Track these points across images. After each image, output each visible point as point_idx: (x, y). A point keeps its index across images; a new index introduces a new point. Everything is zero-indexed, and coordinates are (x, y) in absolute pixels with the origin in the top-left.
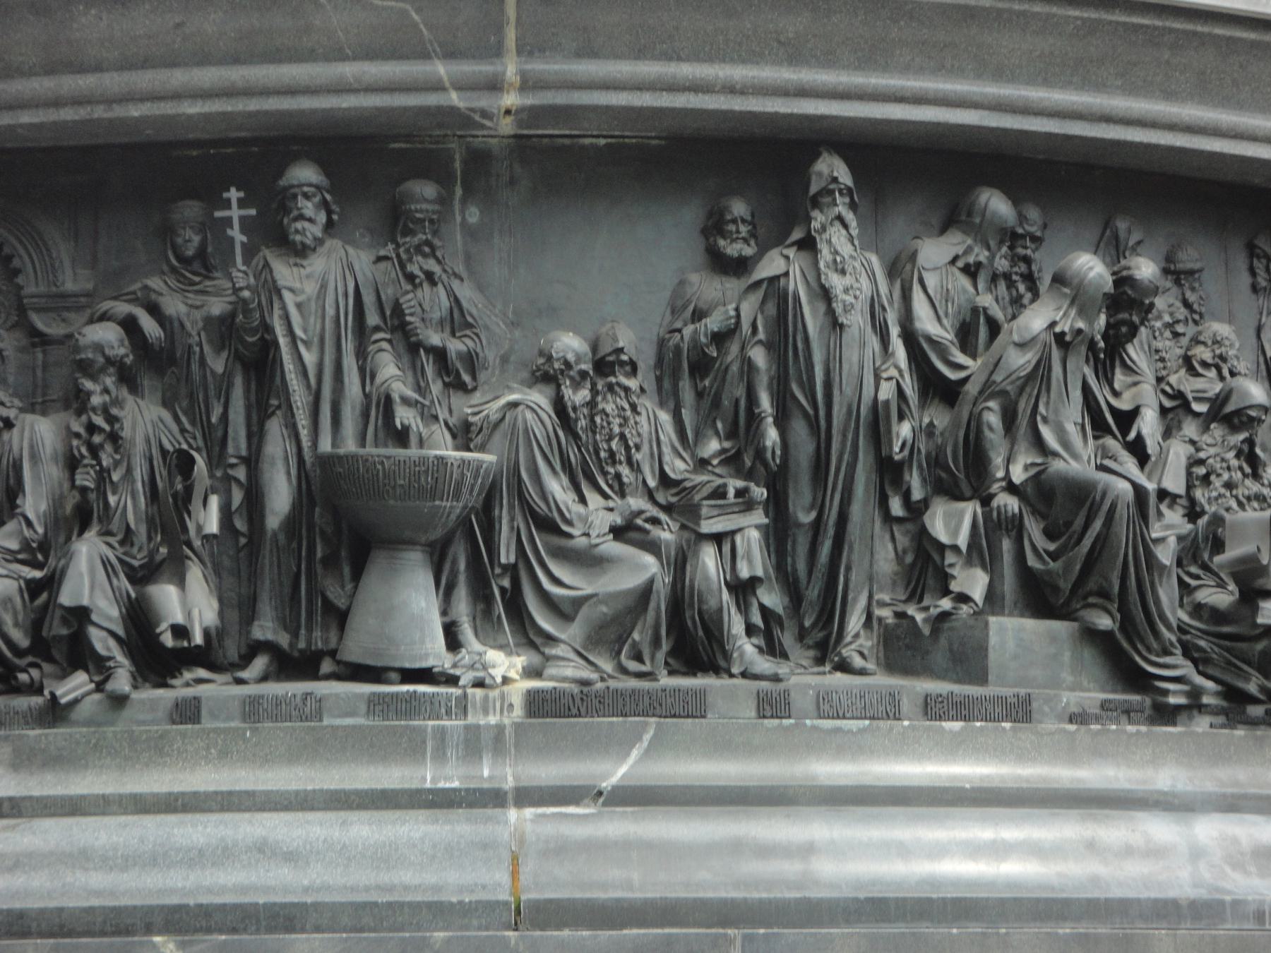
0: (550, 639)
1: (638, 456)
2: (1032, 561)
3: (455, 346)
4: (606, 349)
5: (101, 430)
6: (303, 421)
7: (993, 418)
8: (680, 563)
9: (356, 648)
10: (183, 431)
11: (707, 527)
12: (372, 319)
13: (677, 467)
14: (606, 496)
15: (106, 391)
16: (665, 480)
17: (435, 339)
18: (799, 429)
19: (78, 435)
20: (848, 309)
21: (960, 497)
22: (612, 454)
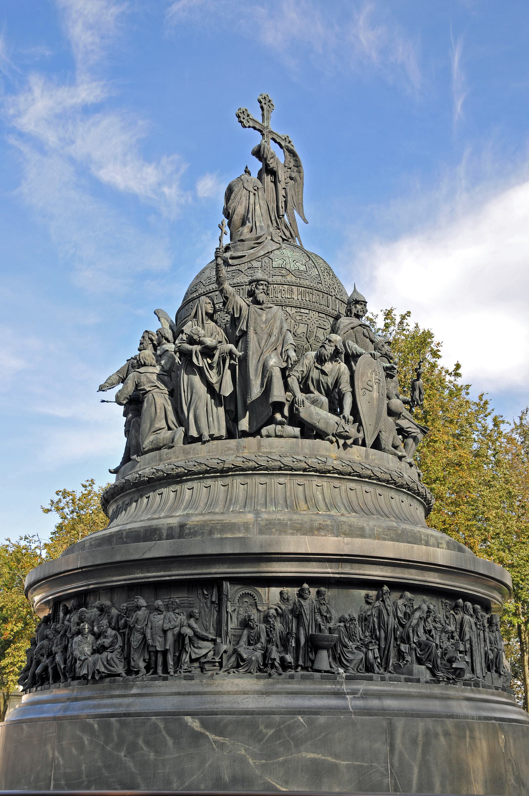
0: (347, 666)
1: (356, 635)
2: (418, 655)
3: (328, 616)
4: (352, 617)
5: (272, 627)
6: (307, 628)
7: (411, 631)
8: (366, 654)
9: (316, 667)
10: (284, 628)
11: (370, 648)
12: (316, 611)
13: (362, 637)
14: (352, 642)
15: (273, 621)
16: (361, 639)
17: (325, 614)
18: (382, 631)
19: (268, 628)
20: (390, 612)
21: (405, 644)
22: (352, 634)
